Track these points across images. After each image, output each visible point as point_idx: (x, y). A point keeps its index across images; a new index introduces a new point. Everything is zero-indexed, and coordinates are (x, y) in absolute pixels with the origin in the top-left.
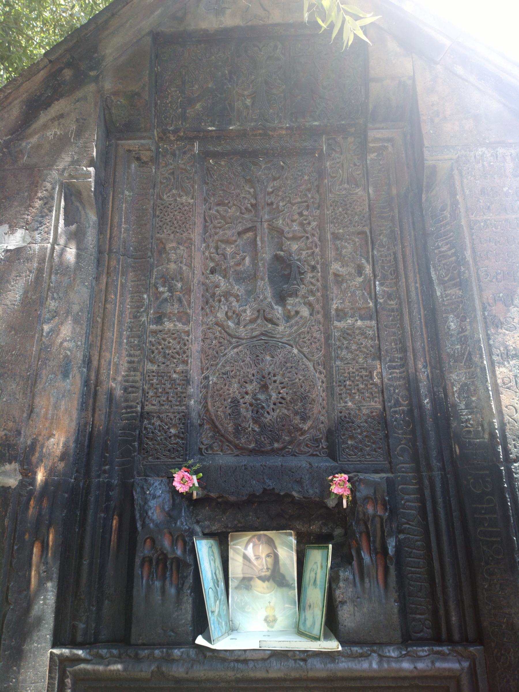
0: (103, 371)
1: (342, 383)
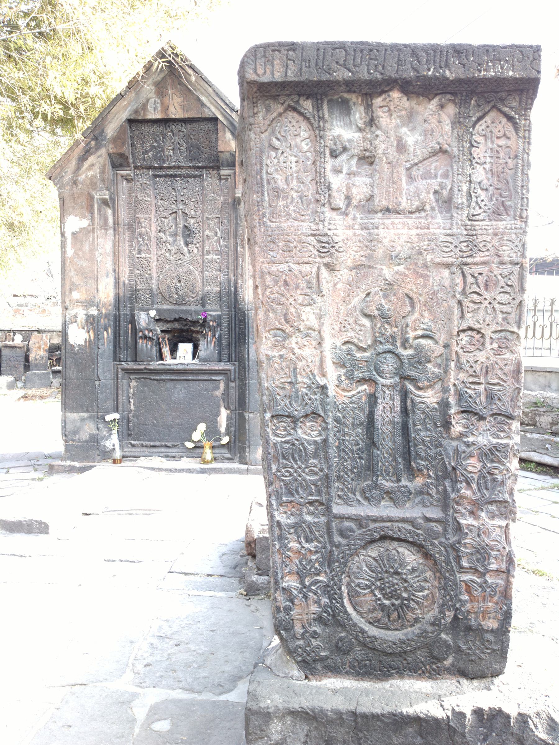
1: (207, 281)
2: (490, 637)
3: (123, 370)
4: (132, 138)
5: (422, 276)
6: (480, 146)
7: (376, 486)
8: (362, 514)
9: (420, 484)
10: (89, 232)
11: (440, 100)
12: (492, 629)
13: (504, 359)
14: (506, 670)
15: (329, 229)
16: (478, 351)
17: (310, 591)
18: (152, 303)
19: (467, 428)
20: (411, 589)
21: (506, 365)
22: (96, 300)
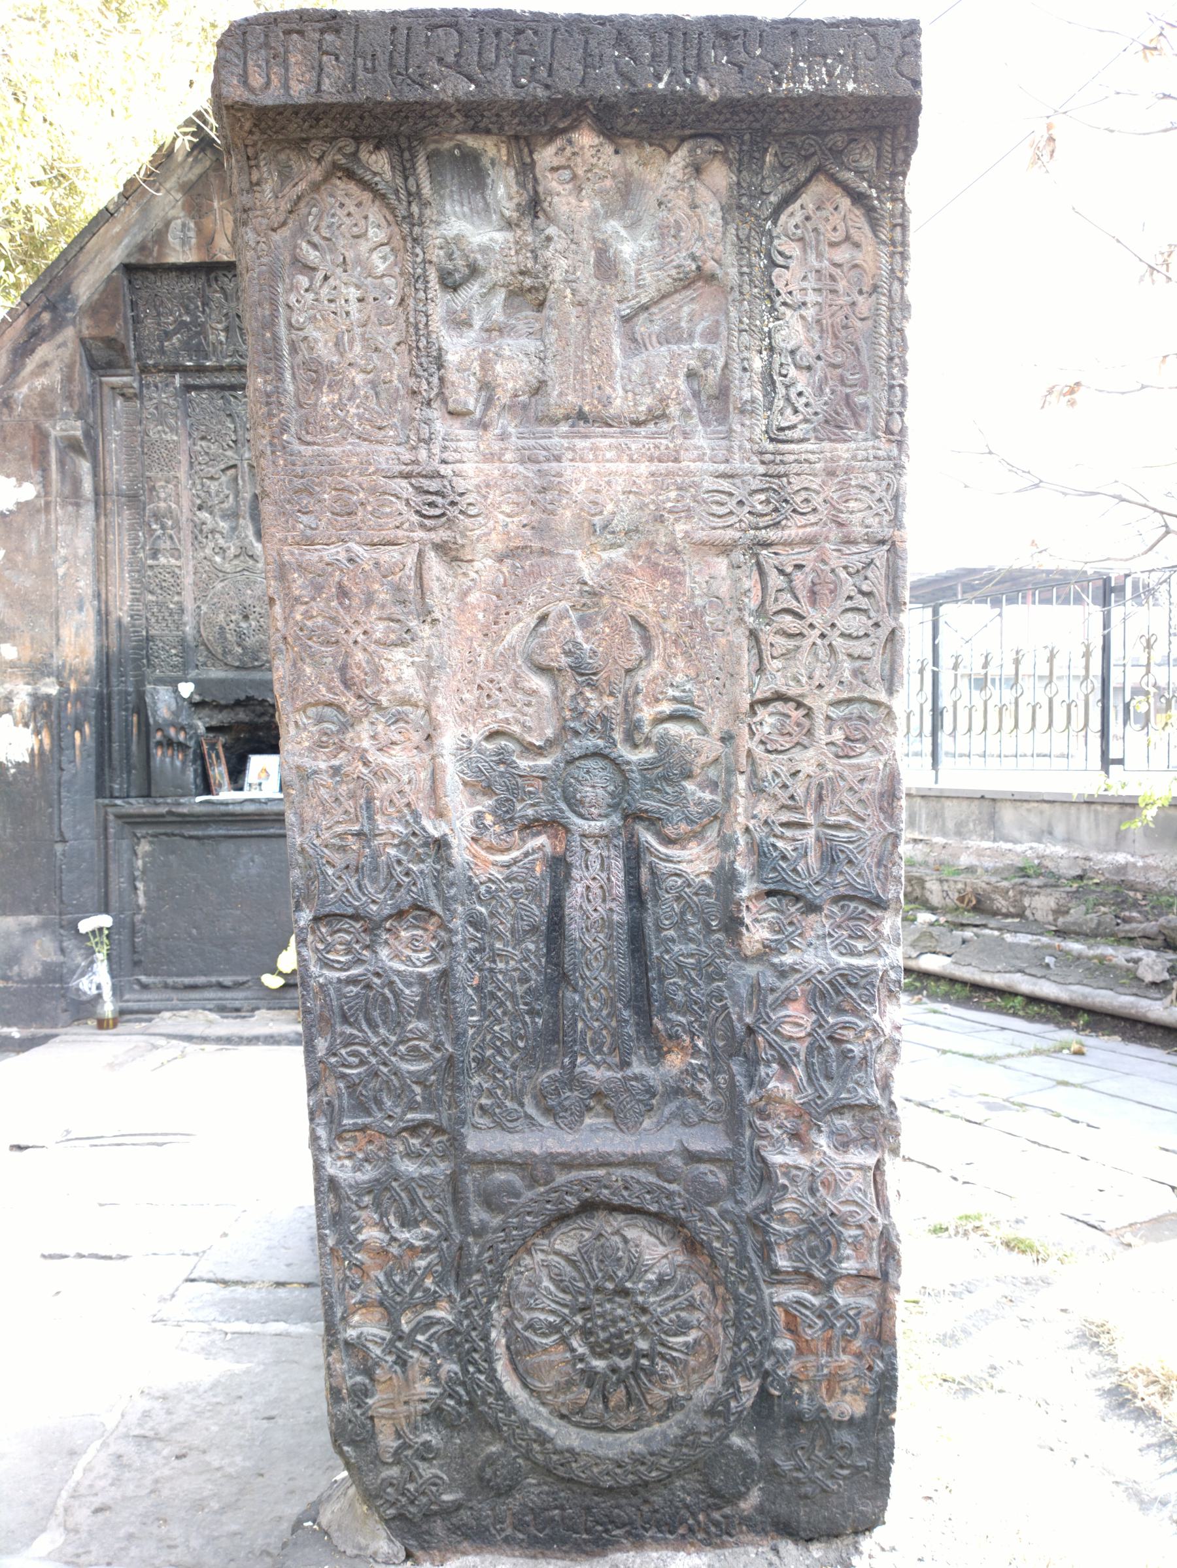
0: (111, 603)
2: (845, 1437)
3: (118, 817)
4: (134, 305)
5: (666, 573)
6: (792, 264)
7: (572, 1080)
8: (537, 1151)
9: (675, 1071)
10: (38, 511)
11: (692, 151)
12: (852, 1418)
13: (859, 767)
14: (888, 1515)
15: (444, 462)
16: (799, 748)
17: (413, 1347)
18: (185, 666)
19: (780, 932)
20: (656, 1329)
21: (861, 781)
22: (56, 662)
